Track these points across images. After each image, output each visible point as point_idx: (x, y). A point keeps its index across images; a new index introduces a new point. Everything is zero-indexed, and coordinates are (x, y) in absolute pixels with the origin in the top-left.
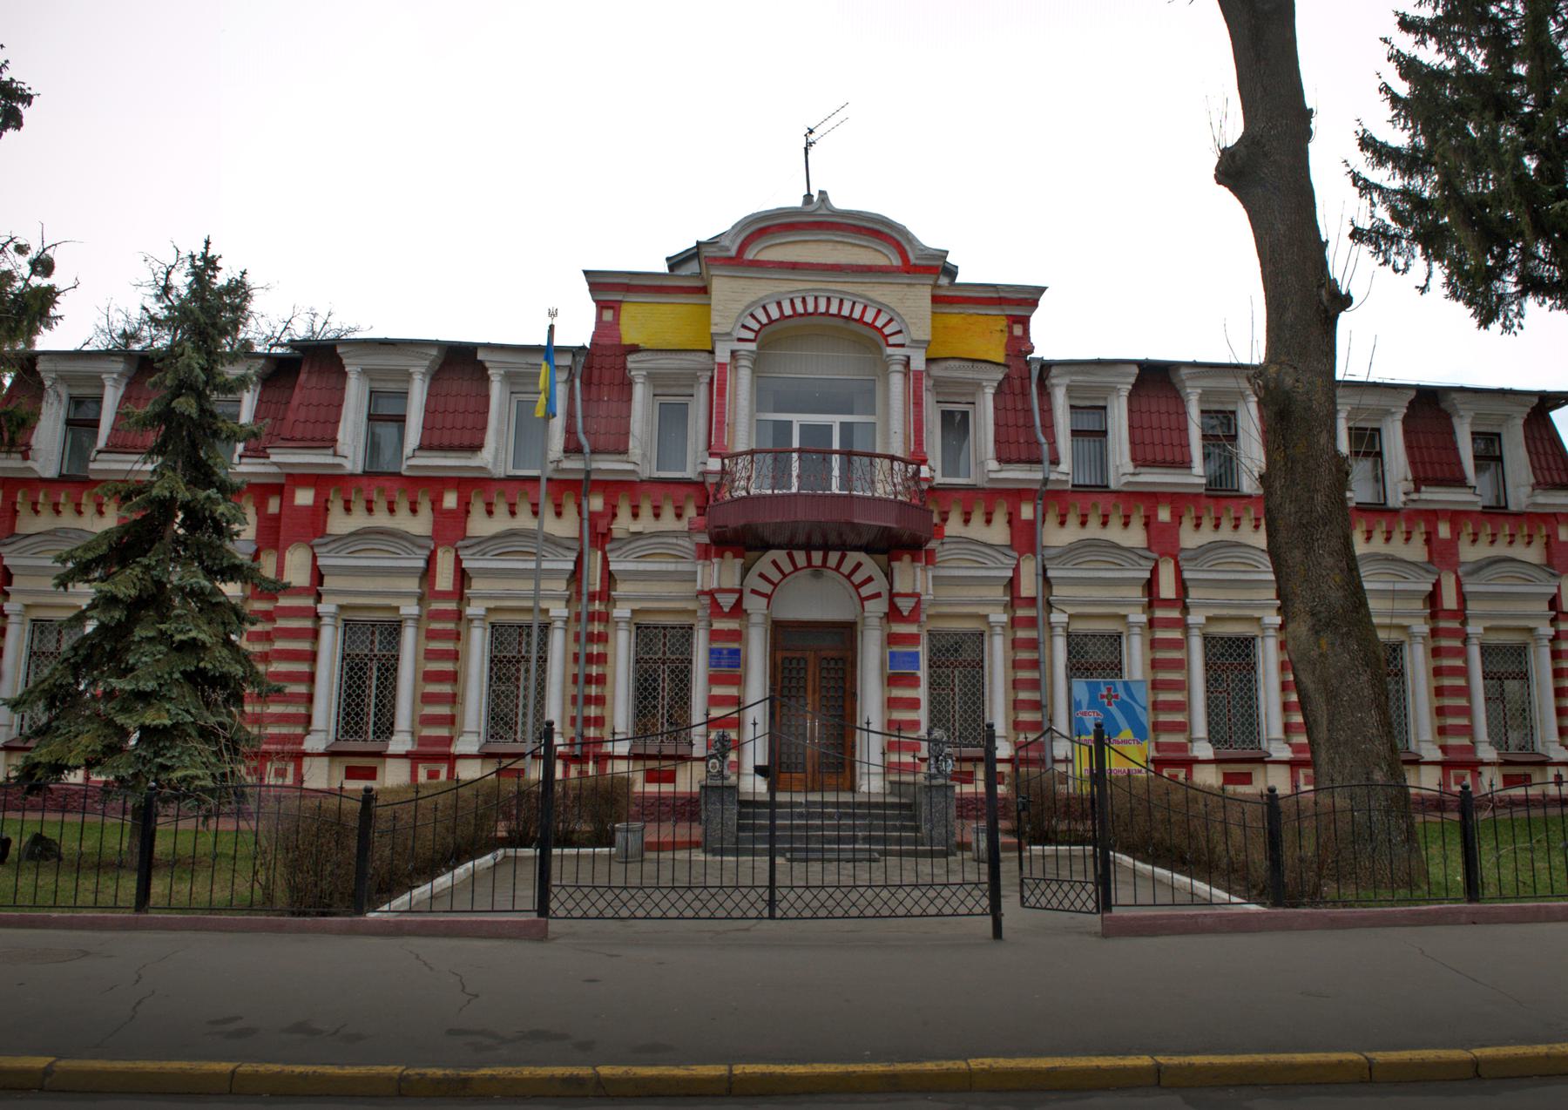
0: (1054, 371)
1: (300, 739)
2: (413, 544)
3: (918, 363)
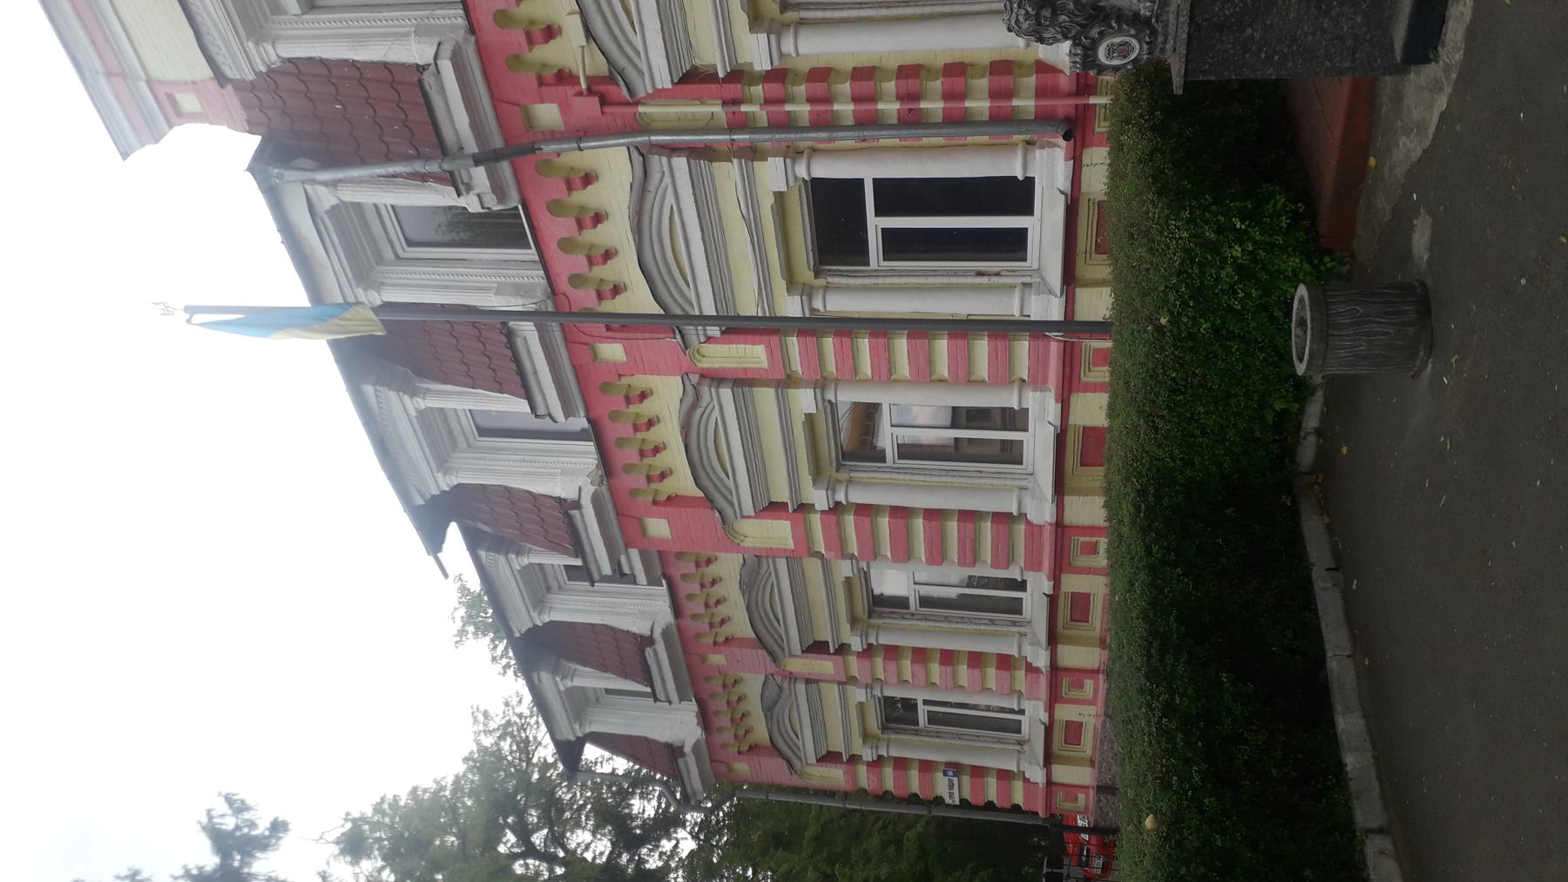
1: (1034, 530)
2: (694, 406)
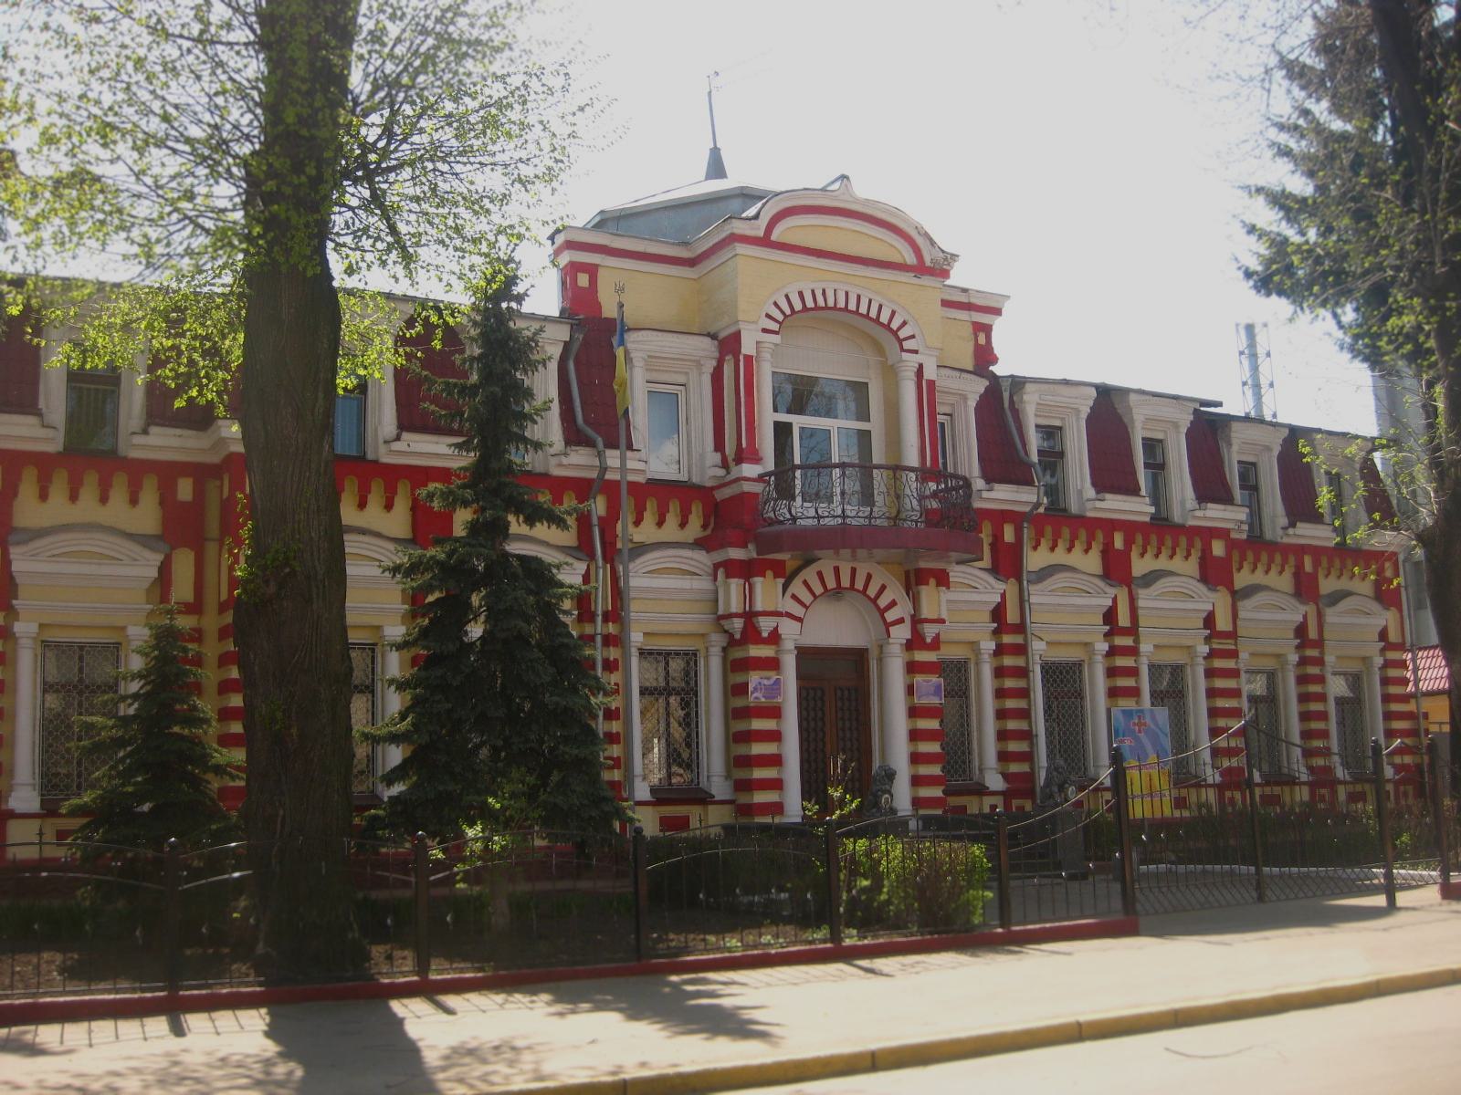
0: (1029, 387)
3: (929, 374)
